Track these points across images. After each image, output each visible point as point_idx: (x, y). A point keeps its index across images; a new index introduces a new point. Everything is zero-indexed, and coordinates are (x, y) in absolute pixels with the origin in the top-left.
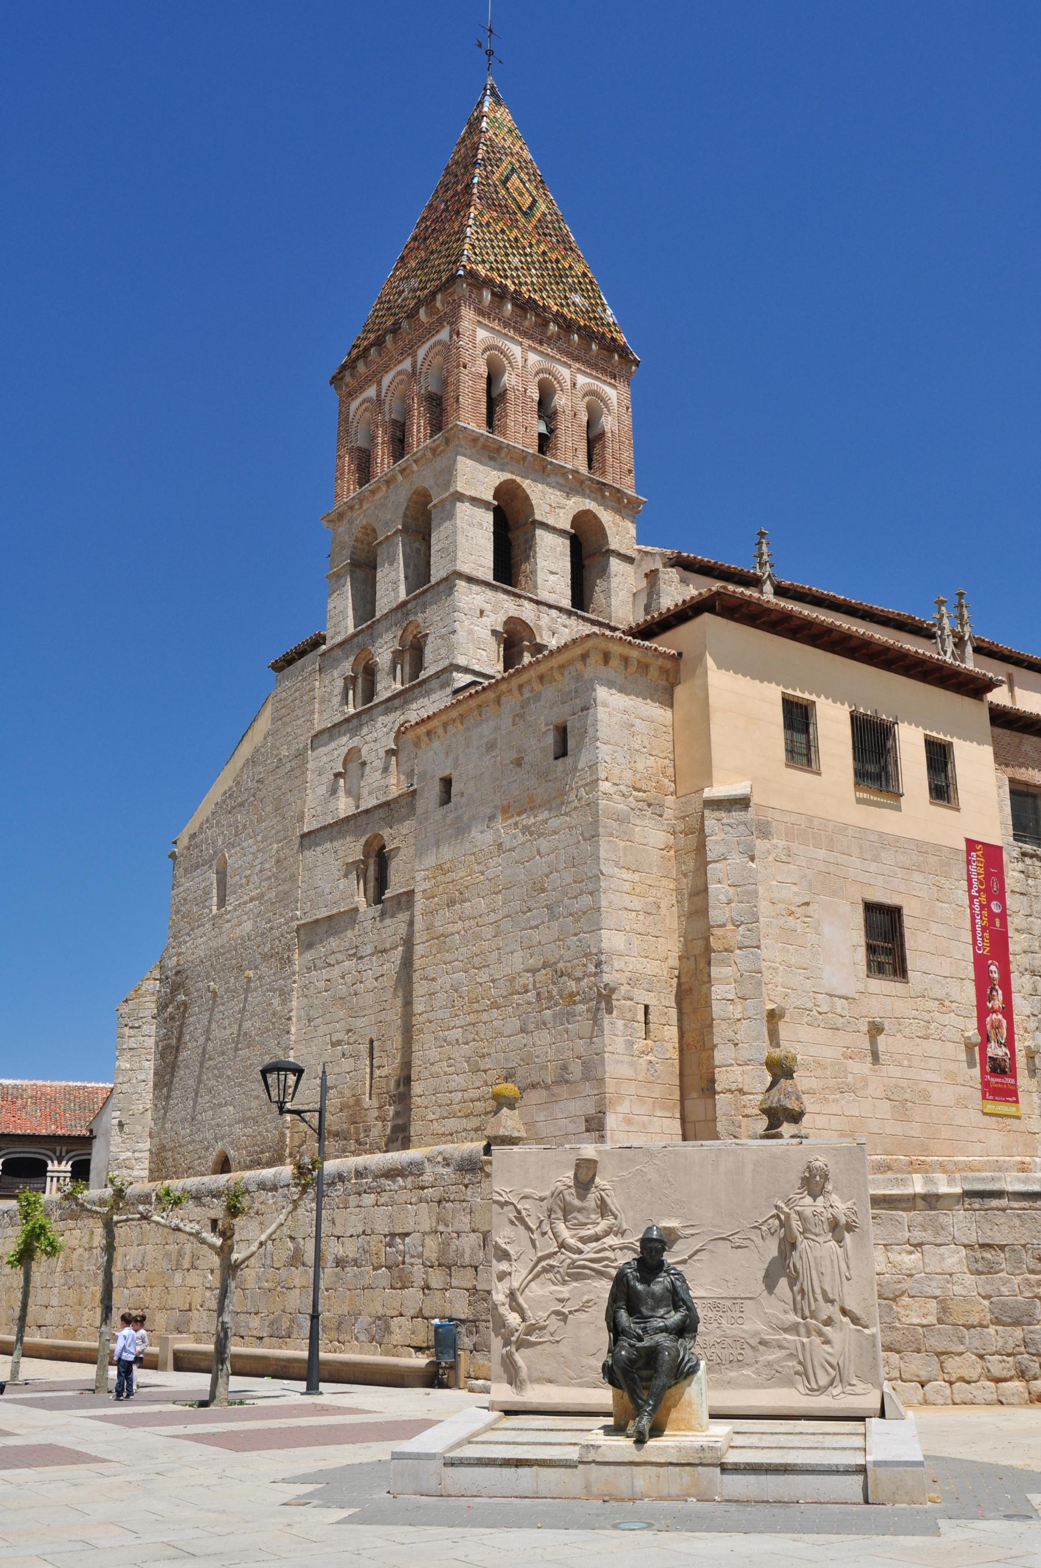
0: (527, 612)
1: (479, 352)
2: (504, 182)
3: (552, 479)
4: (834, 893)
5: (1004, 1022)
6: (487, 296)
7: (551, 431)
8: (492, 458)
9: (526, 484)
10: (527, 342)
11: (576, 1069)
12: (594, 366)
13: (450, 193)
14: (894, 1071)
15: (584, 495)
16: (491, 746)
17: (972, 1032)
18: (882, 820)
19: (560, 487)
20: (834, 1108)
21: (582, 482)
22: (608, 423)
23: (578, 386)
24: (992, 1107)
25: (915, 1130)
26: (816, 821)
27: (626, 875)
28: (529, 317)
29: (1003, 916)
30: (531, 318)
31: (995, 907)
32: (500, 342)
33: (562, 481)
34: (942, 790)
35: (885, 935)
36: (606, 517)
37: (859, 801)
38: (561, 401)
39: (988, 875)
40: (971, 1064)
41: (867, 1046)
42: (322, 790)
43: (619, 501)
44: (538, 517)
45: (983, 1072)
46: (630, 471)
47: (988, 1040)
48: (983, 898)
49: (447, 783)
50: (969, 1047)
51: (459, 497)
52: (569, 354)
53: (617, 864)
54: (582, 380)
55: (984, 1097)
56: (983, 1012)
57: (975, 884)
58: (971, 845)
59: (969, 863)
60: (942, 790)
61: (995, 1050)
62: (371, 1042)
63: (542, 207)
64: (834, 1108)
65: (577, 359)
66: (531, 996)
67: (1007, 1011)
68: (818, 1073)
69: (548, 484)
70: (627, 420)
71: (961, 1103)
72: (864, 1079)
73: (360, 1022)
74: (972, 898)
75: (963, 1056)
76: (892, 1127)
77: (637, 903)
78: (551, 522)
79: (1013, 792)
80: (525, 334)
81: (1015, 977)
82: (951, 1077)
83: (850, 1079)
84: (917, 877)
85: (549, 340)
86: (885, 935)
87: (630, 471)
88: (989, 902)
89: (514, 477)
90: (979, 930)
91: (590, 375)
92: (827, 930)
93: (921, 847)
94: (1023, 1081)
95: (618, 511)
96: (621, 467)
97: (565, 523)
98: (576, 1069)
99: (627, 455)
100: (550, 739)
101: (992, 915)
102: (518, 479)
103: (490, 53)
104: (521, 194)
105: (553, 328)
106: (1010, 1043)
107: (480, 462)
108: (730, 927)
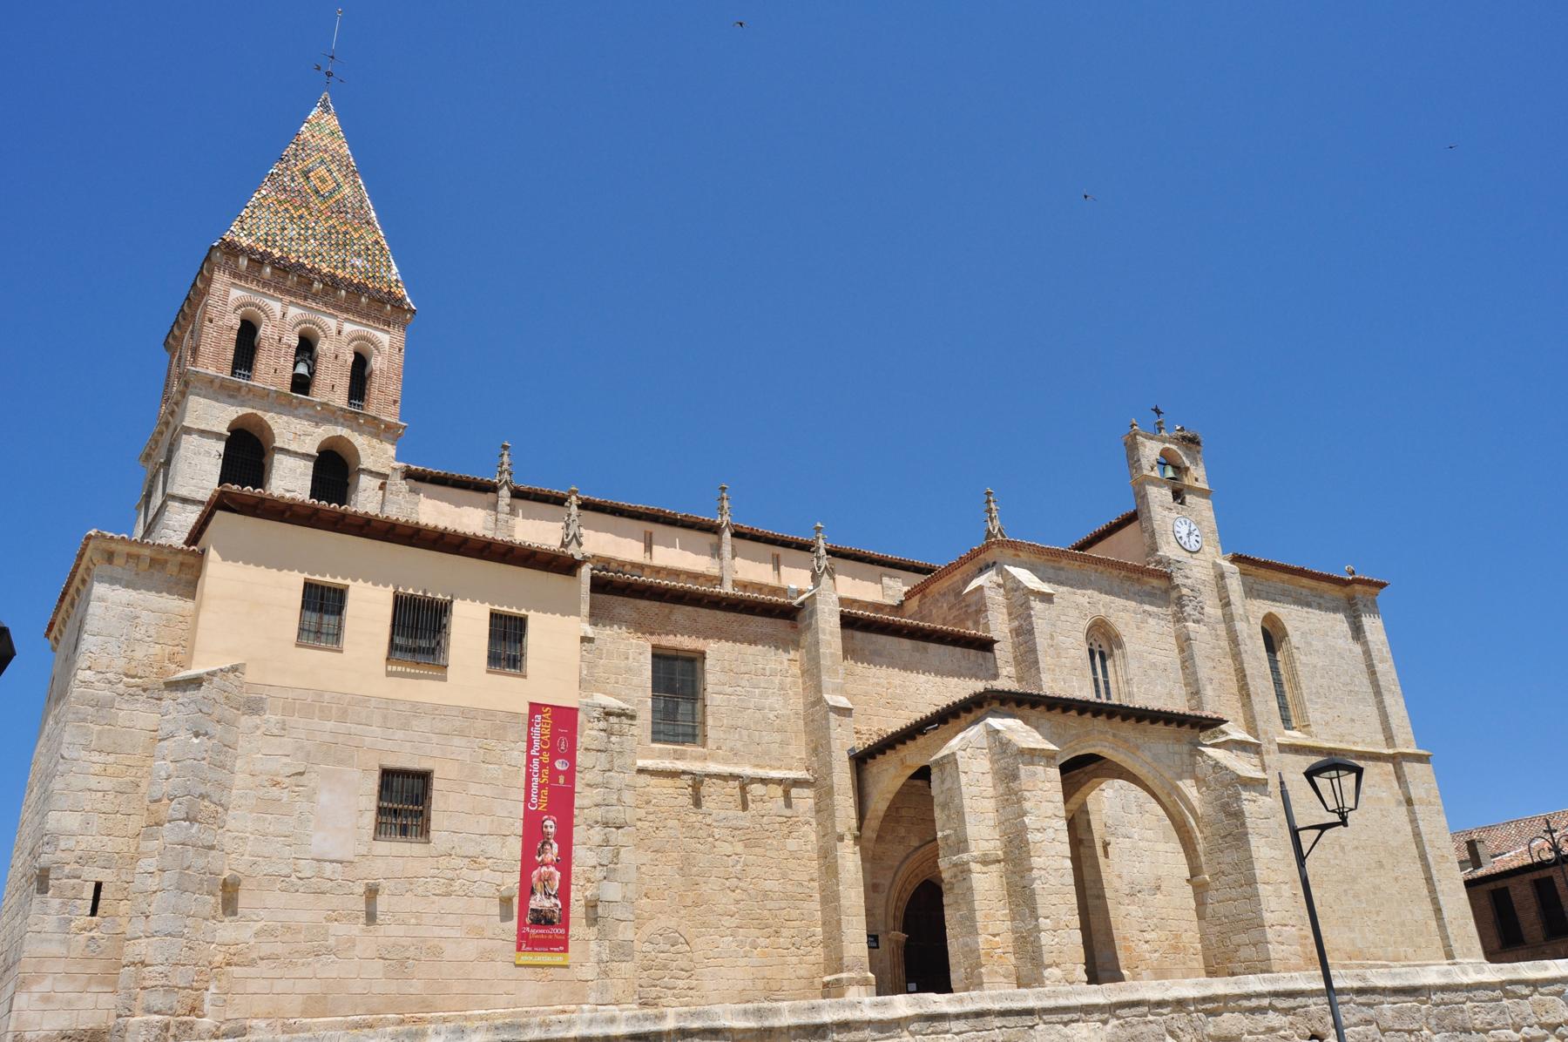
1: (230, 308)
3: (301, 411)
4: (340, 762)
5: (558, 875)
6: (243, 262)
7: (312, 373)
8: (231, 396)
9: (269, 417)
10: (287, 298)
12: (367, 316)
14: (396, 930)
15: (336, 423)
17: (512, 882)
18: (420, 689)
19: (309, 418)
20: (305, 972)
21: (334, 413)
22: (377, 363)
23: (344, 333)
24: (527, 958)
25: (416, 986)
26: (327, 697)
27: (96, 757)
28: (292, 278)
29: (570, 774)
30: (292, 280)
31: (560, 765)
32: (257, 300)
33: (311, 412)
35: (405, 799)
36: (360, 441)
37: (389, 674)
38: (323, 347)
39: (554, 736)
40: (506, 917)
41: (363, 907)
43: (378, 426)
44: (278, 444)
45: (521, 924)
46: (395, 402)
47: (533, 892)
48: (546, 758)
50: (505, 902)
51: (188, 431)
52: (334, 307)
53: (86, 747)
54: (348, 328)
55: (519, 949)
56: (528, 863)
57: (536, 744)
58: (535, 708)
59: (531, 724)
61: (538, 902)
63: (347, 190)
64: (305, 972)
65: (347, 311)
67: (564, 863)
68: (288, 937)
69: (295, 416)
70: (399, 359)
71: (486, 956)
72: (352, 942)
74: (530, 759)
75: (497, 910)
76: (393, 987)
77: (107, 783)
78: (293, 447)
79: (654, 656)
80: (288, 292)
81: (579, 834)
82: (478, 933)
83: (332, 941)
84: (457, 741)
85: (315, 297)
86: (405, 799)
87: (395, 402)
88: (552, 761)
89: (250, 411)
90: (535, 787)
91: (360, 324)
92: (324, 798)
93: (467, 714)
94: (578, 928)
95: (376, 436)
96: (384, 400)
99: (394, 389)
101: (555, 773)
102: (260, 413)
103: (329, 74)
105: (317, 286)
106: (564, 894)
107: (217, 400)
108: (165, 801)
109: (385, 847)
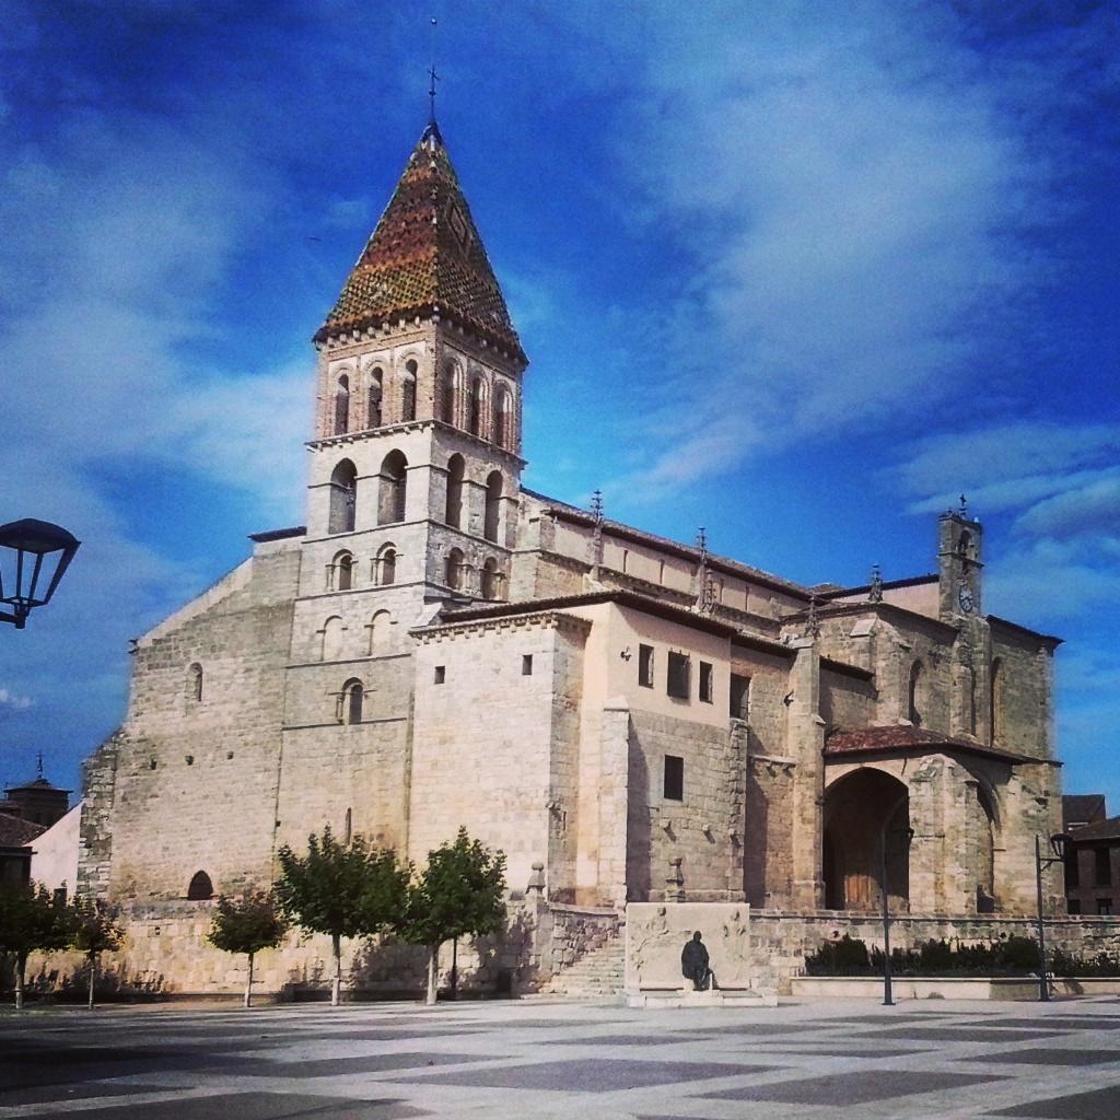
0: (462, 544)
2: (449, 219)
6: (450, 324)
11: (528, 846)
13: (409, 217)
16: (477, 657)
34: (705, 695)
42: (306, 639)
49: (441, 670)
60: (705, 695)
62: (349, 810)
66: (501, 804)
73: (339, 797)
84: (690, 742)
97: (484, 484)
98: (528, 846)
100: (521, 661)
104: (459, 228)
109: (669, 802)
